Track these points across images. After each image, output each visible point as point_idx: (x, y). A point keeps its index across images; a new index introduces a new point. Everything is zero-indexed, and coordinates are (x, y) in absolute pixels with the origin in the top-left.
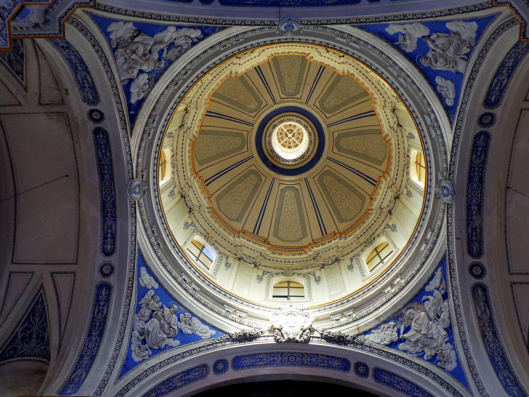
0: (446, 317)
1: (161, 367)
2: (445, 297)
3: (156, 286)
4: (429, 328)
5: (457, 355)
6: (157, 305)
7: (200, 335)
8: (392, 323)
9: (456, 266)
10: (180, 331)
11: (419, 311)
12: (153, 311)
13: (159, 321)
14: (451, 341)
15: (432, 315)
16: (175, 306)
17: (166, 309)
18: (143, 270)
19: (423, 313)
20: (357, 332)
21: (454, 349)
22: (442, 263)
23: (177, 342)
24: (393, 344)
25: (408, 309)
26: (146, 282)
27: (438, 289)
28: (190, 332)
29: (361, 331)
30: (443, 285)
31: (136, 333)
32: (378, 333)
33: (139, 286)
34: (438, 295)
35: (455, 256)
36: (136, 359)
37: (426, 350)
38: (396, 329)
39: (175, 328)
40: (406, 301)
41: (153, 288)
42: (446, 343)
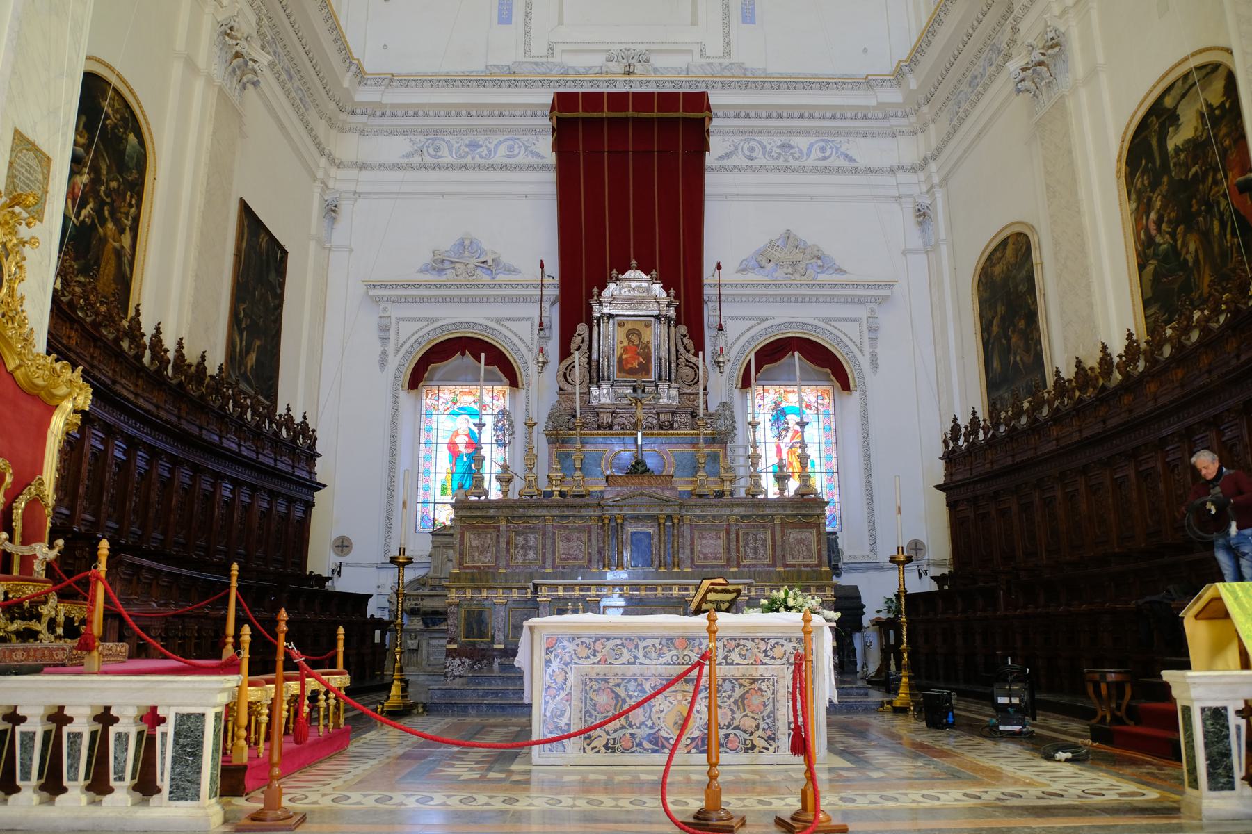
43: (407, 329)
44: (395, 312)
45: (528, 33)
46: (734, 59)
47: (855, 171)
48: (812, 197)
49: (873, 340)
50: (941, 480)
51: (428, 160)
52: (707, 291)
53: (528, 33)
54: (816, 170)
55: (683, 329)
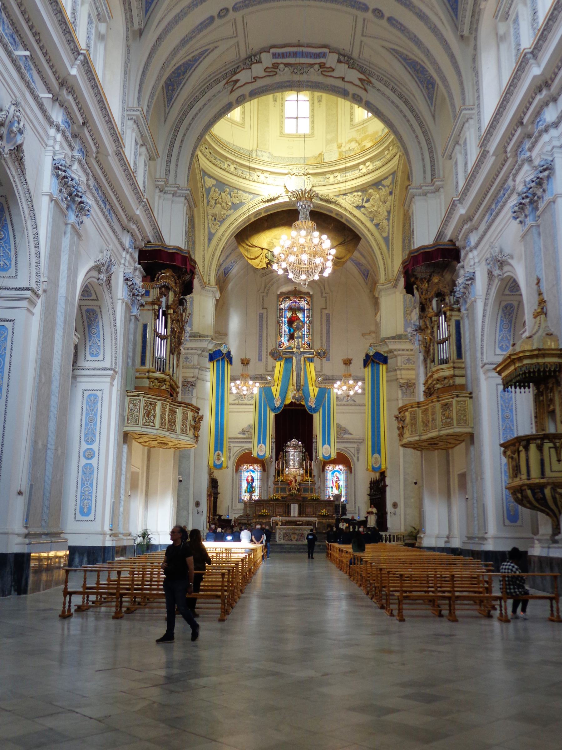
0: (389, 205)
1: (226, 231)
2: (391, 193)
3: (214, 182)
4: (379, 207)
5: (389, 230)
6: (217, 195)
7: (244, 201)
8: (360, 193)
9: (399, 183)
10: (233, 203)
11: (376, 193)
12: (216, 200)
13: (221, 204)
14: (388, 220)
15: (382, 200)
16: (228, 190)
17: (223, 194)
18: (206, 178)
19: (378, 196)
20: (339, 193)
21: (389, 225)
22: (394, 174)
23: (232, 211)
24: (358, 207)
25: (370, 188)
26: (209, 185)
27: (388, 187)
28: (238, 202)
29: (342, 193)
30: (391, 186)
31: (210, 217)
32: (351, 197)
33: (206, 188)
34: (388, 190)
35: (399, 178)
36: (213, 231)
37: (375, 219)
38: (361, 198)
39: (230, 204)
40: (370, 184)
41: (213, 185)
42: (386, 219)
43: (237, 449)
44: (232, 445)
45: (266, 364)
46: (323, 373)
47: (355, 405)
48: (343, 413)
49: (358, 453)
50: (369, 493)
51: (240, 402)
52: (314, 440)
53: (266, 364)
54: (344, 405)
55: (307, 453)
